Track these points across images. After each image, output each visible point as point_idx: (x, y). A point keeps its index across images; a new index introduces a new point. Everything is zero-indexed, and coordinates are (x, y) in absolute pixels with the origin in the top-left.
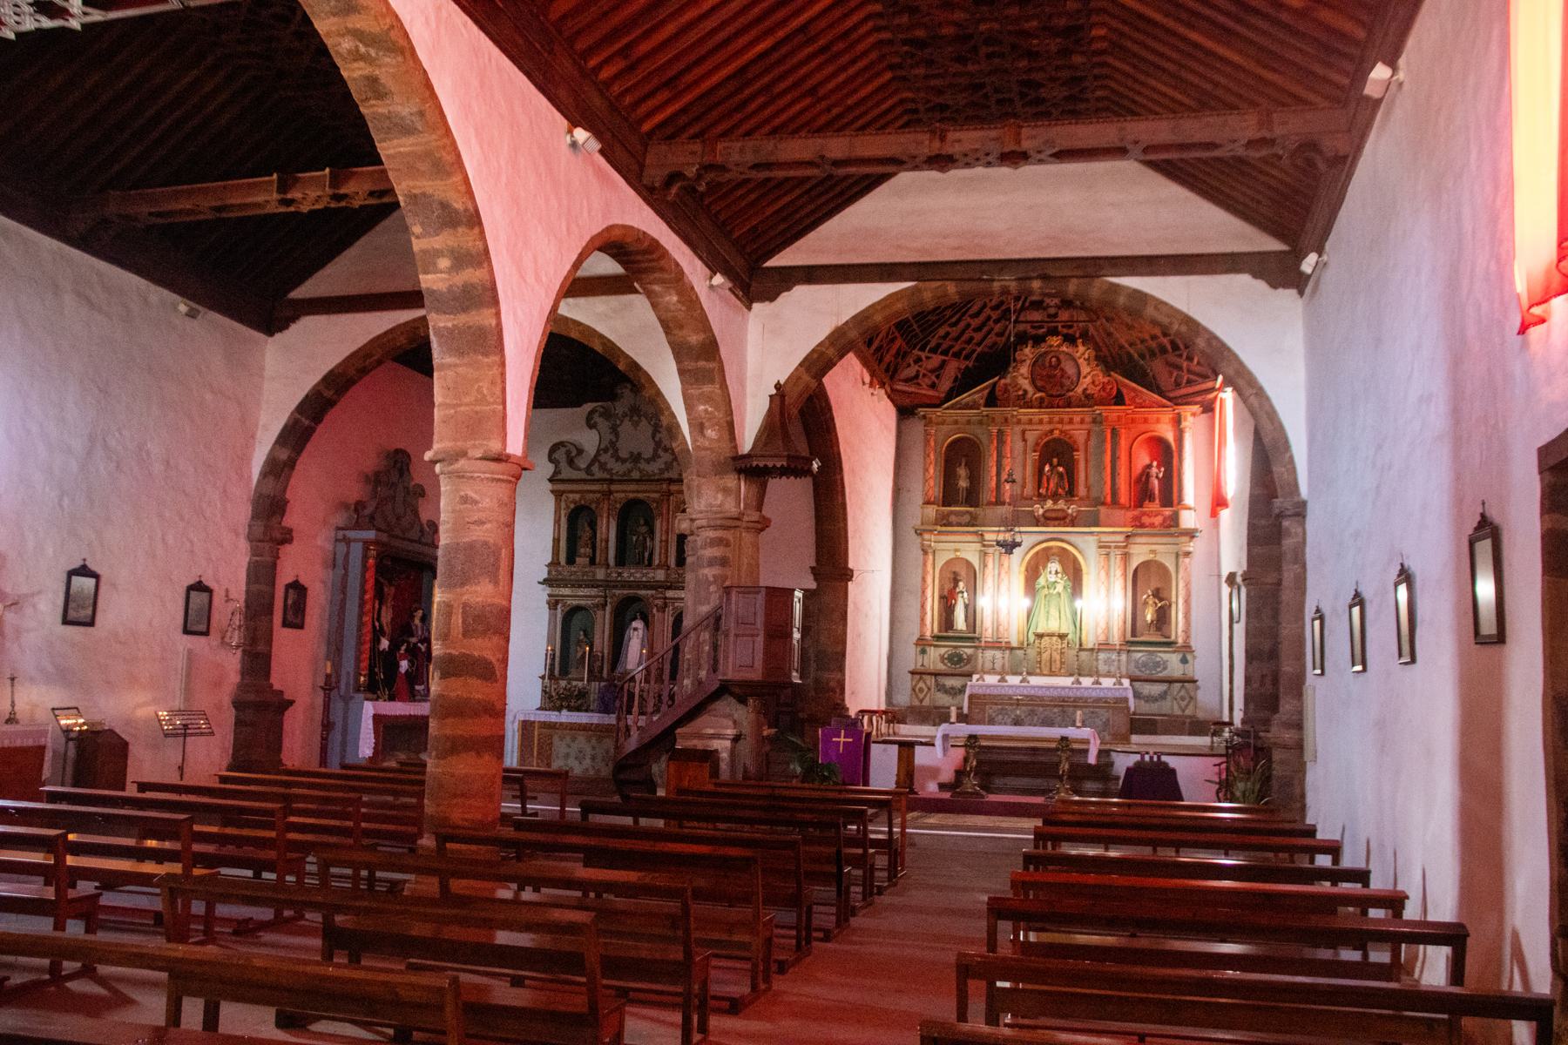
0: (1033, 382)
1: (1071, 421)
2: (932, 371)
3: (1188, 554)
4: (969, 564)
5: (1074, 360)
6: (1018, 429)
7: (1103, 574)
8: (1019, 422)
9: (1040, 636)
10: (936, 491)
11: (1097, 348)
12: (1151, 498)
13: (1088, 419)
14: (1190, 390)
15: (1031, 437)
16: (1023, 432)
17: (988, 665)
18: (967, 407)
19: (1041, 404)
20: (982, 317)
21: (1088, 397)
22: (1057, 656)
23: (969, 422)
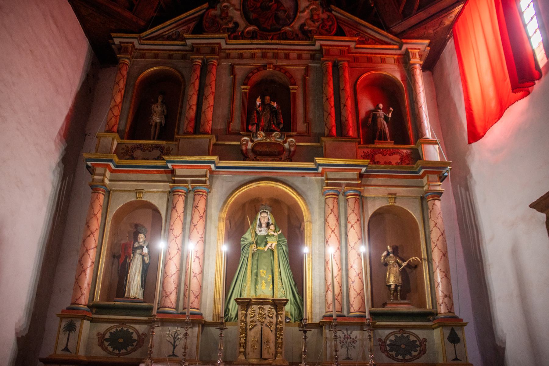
0: (245, 15)
1: (287, 57)
3: (439, 194)
4: (156, 210)
6: (225, 63)
7: (332, 219)
8: (228, 56)
9: (245, 304)
10: (125, 125)
12: (382, 137)
13: (305, 55)
14: (423, 15)
15: (240, 72)
16: (232, 67)
17: (167, 350)
18: (170, 38)
19: (253, 36)
22: (269, 334)
23: (170, 57)
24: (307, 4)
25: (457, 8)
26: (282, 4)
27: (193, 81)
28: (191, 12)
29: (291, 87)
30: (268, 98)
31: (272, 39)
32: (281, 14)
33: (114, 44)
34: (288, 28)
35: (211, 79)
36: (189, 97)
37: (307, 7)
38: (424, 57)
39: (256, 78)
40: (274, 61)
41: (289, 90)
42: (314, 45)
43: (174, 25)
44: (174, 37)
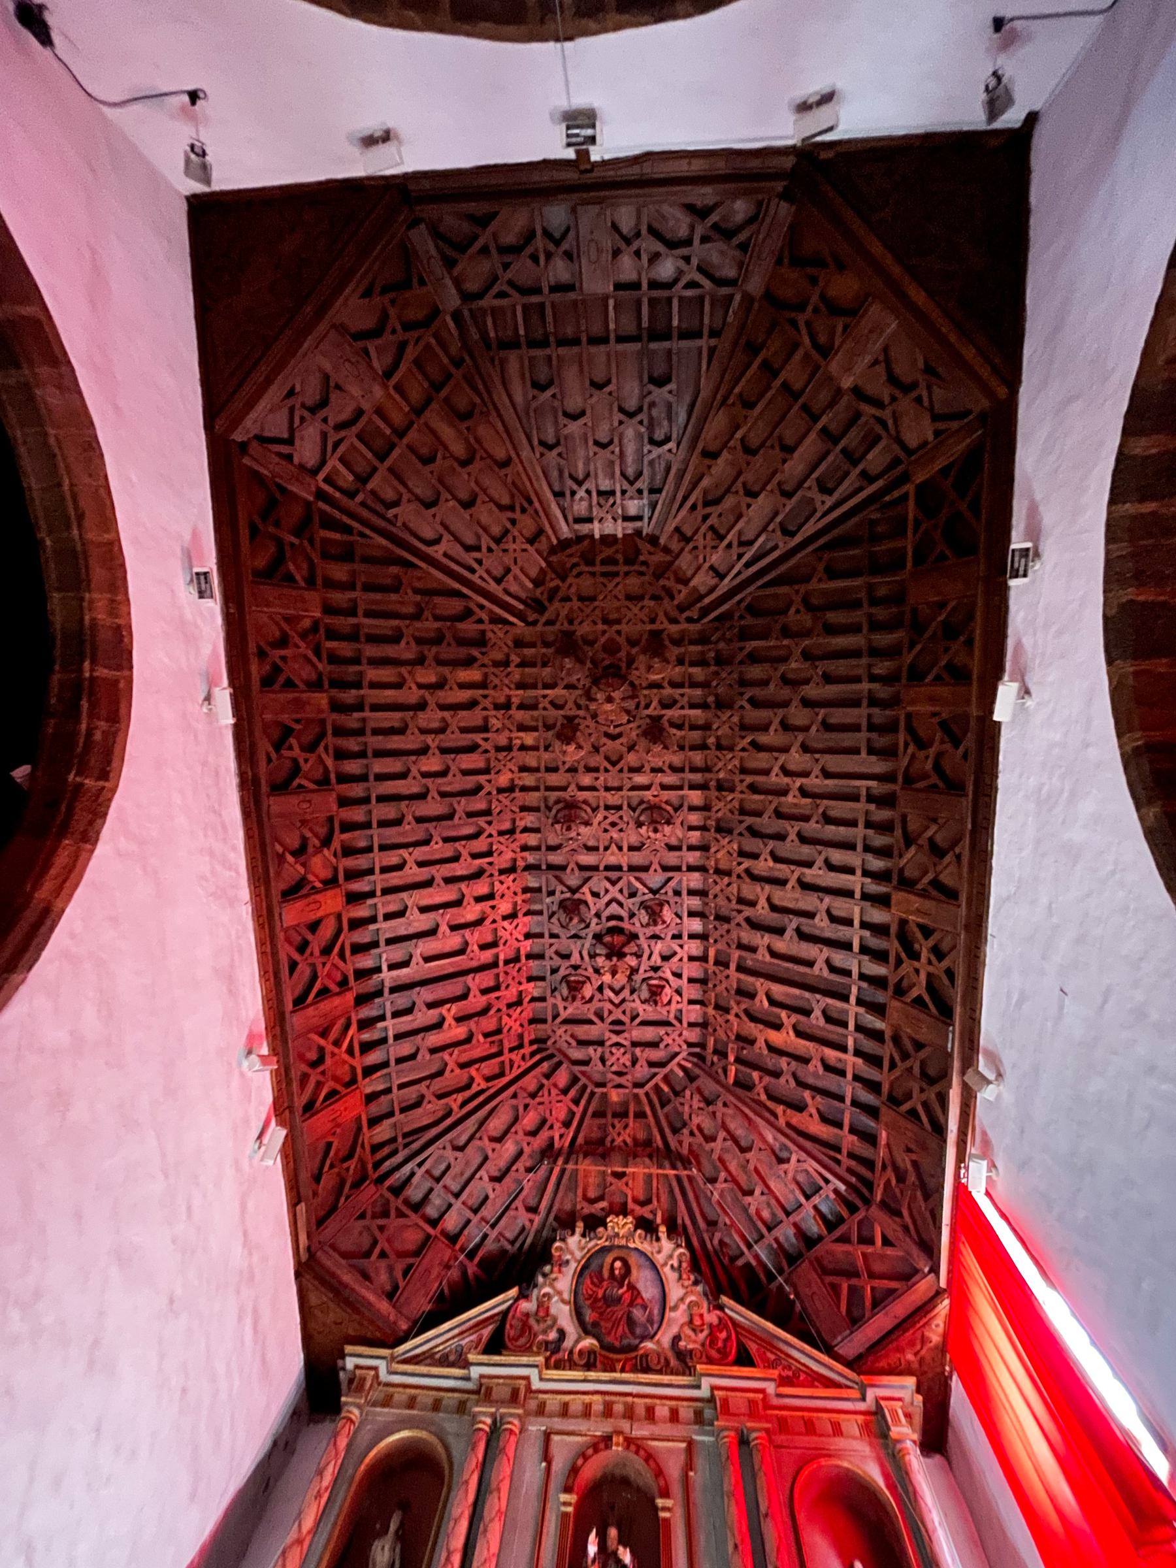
0: (578, 1314)
1: (650, 1413)
2: (401, 1255)
5: (654, 1266)
6: (536, 1427)
8: (541, 1411)
11: (689, 1246)
13: (686, 1412)
15: (563, 1449)
16: (547, 1436)
18: (444, 1361)
19: (589, 1362)
20: (509, 1148)
21: (681, 1355)
23: (436, 1406)
24: (681, 1292)
25: (940, 1307)
26: (639, 1293)
27: (465, 1477)
29: (660, 1502)
30: (613, 1532)
31: (623, 1370)
32: (637, 1313)
33: (344, 1369)
34: (649, 1345)
35: (502, 1470)
36: (452, 1524)
37: (682, 1299)
38: (918, 1419)
39: (591, 1470)
40: (625, 1425)
41: (656, 1509)
42: (698, 1387)
43: (456, 1331)
44: (452, 1358)
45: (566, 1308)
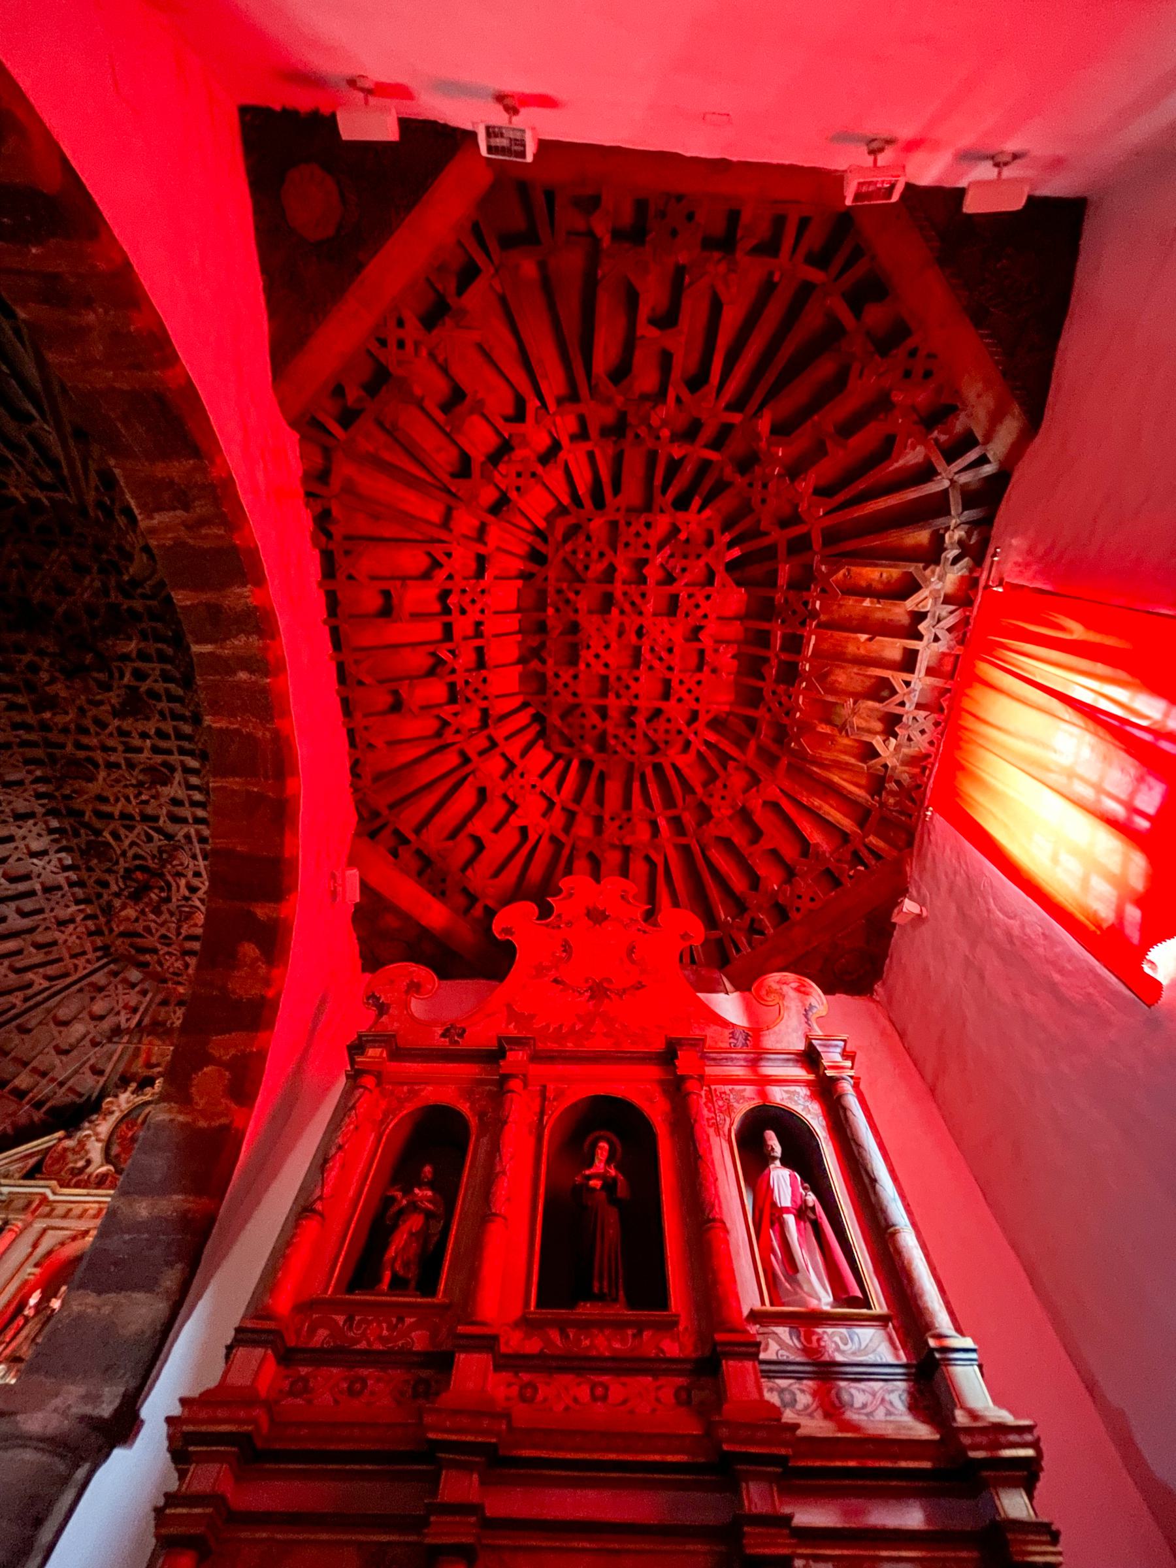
28: (39, 1141)
45: (99, 1145)
